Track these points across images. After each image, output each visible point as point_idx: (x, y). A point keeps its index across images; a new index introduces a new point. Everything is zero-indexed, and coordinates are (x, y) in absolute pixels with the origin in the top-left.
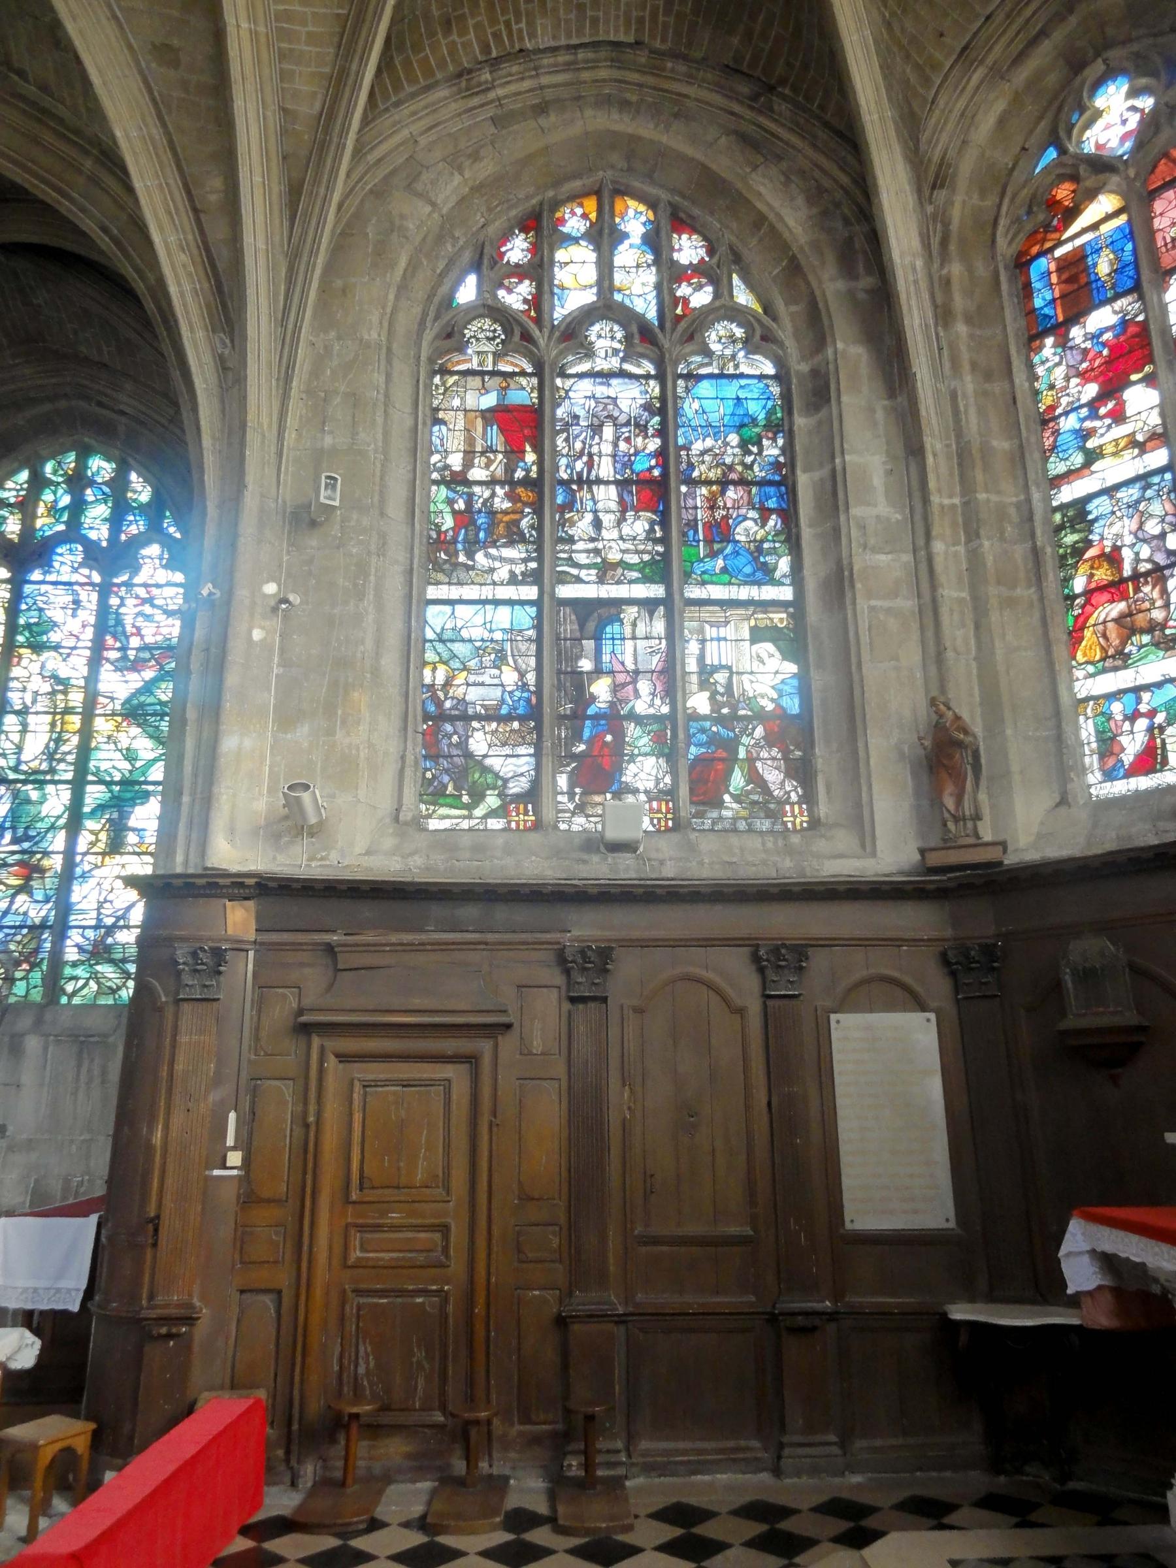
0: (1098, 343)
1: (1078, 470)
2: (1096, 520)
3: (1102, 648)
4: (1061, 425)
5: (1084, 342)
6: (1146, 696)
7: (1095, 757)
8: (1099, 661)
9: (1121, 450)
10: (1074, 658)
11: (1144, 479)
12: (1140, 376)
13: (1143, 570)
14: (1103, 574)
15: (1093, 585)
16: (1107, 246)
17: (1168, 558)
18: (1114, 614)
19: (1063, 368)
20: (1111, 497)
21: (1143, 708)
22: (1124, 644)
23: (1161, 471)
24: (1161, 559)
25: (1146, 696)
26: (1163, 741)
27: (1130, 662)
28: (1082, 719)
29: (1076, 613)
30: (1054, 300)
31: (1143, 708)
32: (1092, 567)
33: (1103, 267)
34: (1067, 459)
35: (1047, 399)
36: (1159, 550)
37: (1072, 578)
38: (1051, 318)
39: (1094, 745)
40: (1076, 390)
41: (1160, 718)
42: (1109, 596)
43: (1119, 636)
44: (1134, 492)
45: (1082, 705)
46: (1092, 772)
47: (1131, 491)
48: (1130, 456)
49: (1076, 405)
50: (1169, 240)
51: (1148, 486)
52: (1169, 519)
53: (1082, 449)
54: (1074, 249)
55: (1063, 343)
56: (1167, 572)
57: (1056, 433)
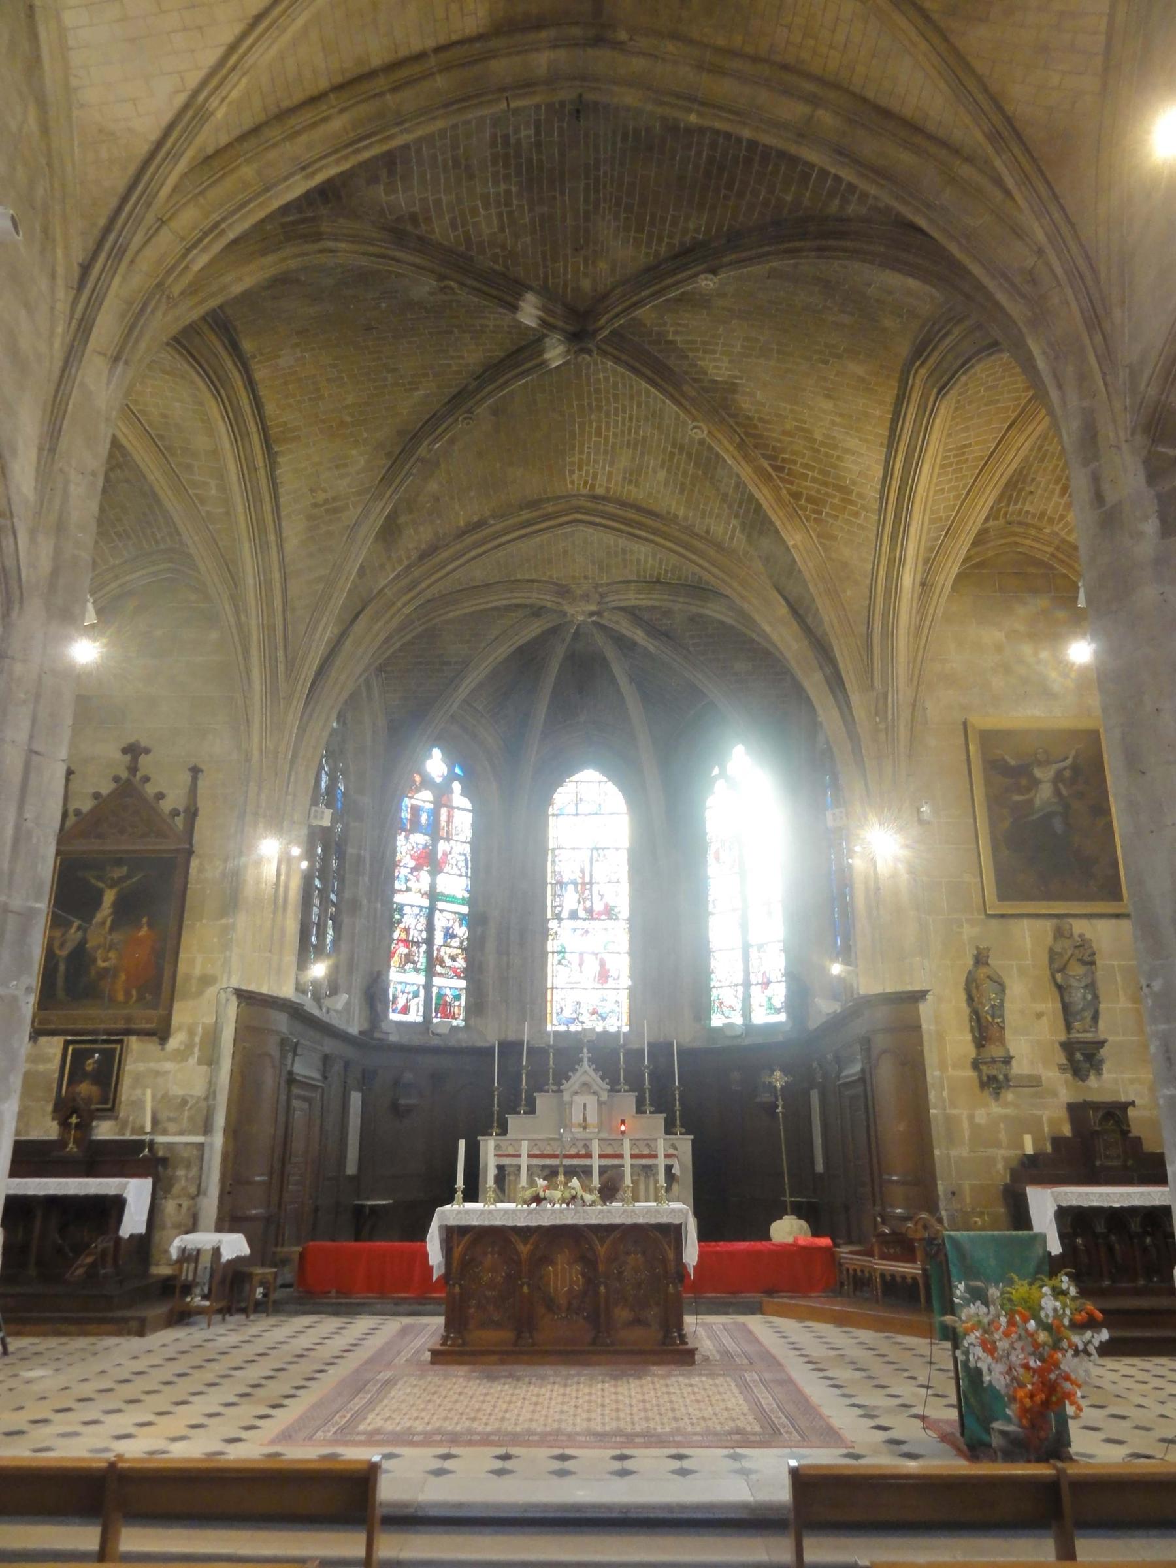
11: (421, 907)
14: (403, 936)
21: (407, 991)
30: (406, 819)
31: (407, 991)
33: (424, 818)
44: (417, 910)
55: (407, 838)
57: (399, 873)
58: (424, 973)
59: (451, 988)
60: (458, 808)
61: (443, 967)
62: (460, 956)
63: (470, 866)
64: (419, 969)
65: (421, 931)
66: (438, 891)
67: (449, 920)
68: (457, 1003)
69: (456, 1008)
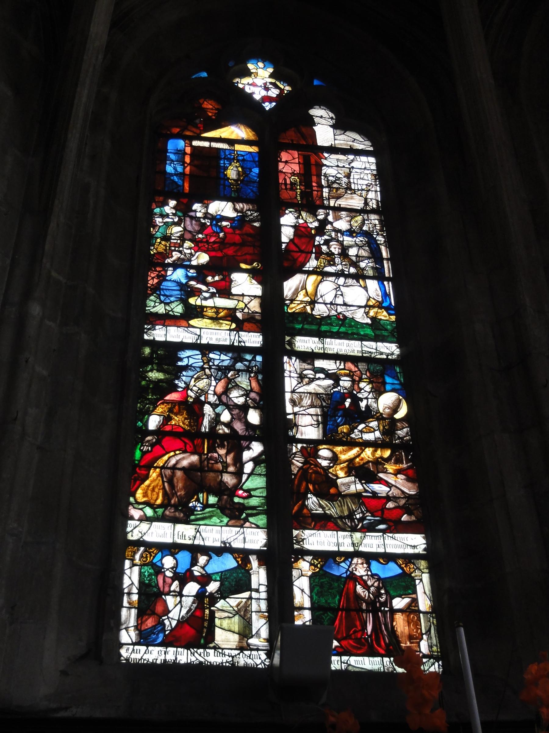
0: (216, 225)
1: (175, 317)
2: (186, 368)
3: (165, 494)
4: (169, 273)
5: (204, 218)
6: (202, 560)
7: (134, 612)
8: (159, 506)
9: (221, 318)
10: (134, 496)
12: (248, 267)
13: (221, 431)
14: (178, 420)
15: (168, 428)
16: (238, 161)
17: (247, 430)
18: (185, 463)
19: (179, 229)
20: (204, 355)
21: (197, 571)
22: (189, 496)
23: (253, 351)
24: (238, 427)
25: (202, 560)
26: (212, 613)
27: (192, 517)
28: (127, 563)
29: (145, 449)
30: (182, 175)
31: (197, 571)
32: (171, 410)
34: (168, 304)
35: (159, 246)
36: (240, 420)
37: (149, 413)
38: (179, 186)
39: (135, 598)
40: (189, 251)
41: (213, 587)
42: (182, 445)
43: (185, 487)
44: (225, 359)
45: (130, 549)
46: (127, 629)
47: (223, 357)
48: (228, 327)
49: (188, 263)
50: (288, 182)
51: (242, 360)
52: (253, 395)
53: (184, 301)
54: (210, 148)
56: (244, 444)
57: (163, 278)
58: (262, 520)
59: (369, 557)
60: (333, 150)
61: (331, 498)
62: (391, 468)
63: (385, 253)
64: (242, 508)
65: (244, 408)
66: (295, 308)
67: (335, 378)
68: (399, 603)
69: (400, 619)
